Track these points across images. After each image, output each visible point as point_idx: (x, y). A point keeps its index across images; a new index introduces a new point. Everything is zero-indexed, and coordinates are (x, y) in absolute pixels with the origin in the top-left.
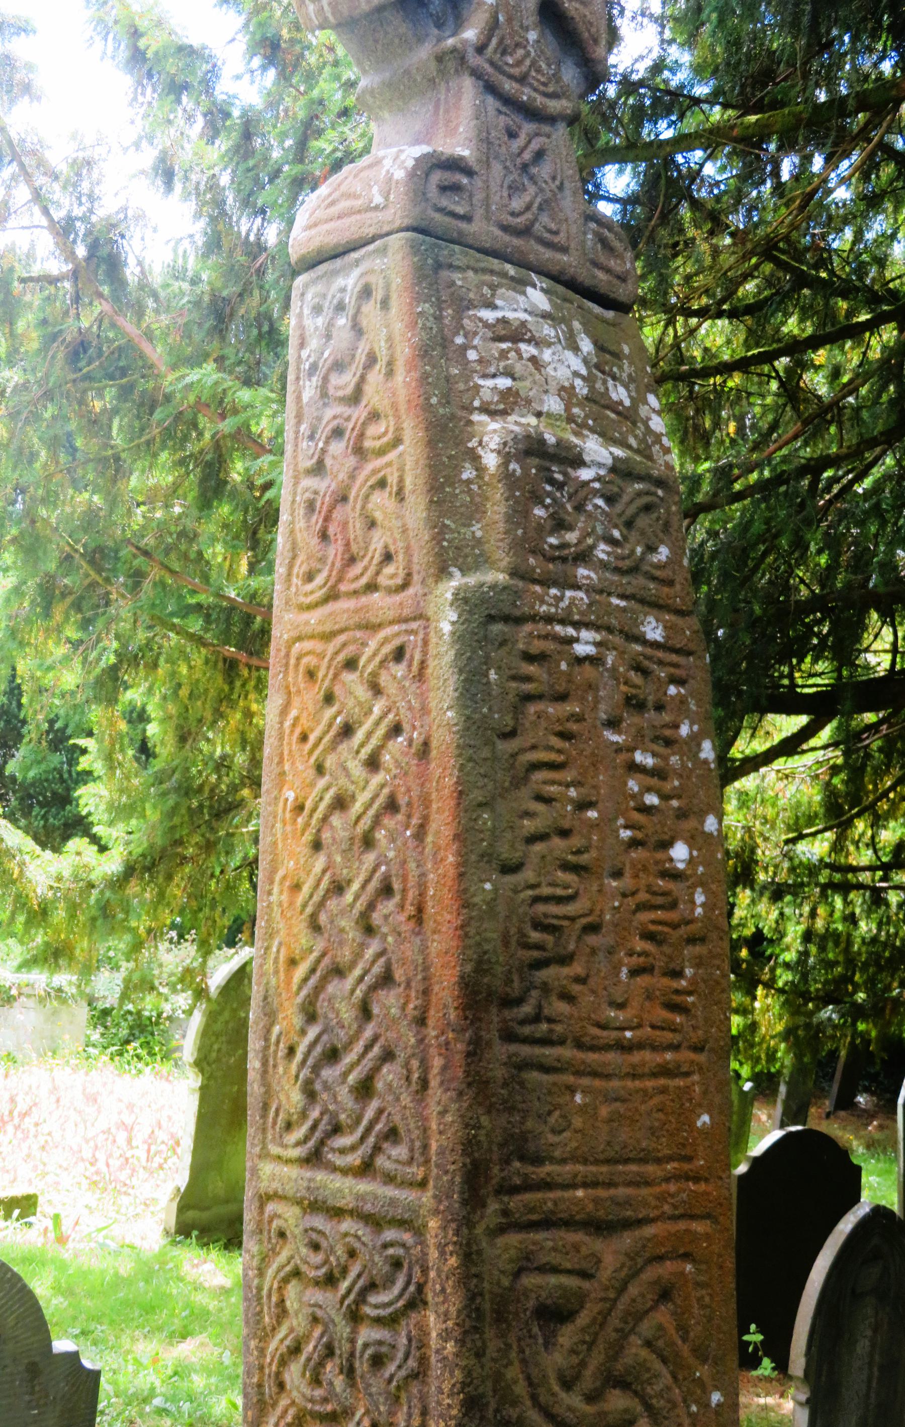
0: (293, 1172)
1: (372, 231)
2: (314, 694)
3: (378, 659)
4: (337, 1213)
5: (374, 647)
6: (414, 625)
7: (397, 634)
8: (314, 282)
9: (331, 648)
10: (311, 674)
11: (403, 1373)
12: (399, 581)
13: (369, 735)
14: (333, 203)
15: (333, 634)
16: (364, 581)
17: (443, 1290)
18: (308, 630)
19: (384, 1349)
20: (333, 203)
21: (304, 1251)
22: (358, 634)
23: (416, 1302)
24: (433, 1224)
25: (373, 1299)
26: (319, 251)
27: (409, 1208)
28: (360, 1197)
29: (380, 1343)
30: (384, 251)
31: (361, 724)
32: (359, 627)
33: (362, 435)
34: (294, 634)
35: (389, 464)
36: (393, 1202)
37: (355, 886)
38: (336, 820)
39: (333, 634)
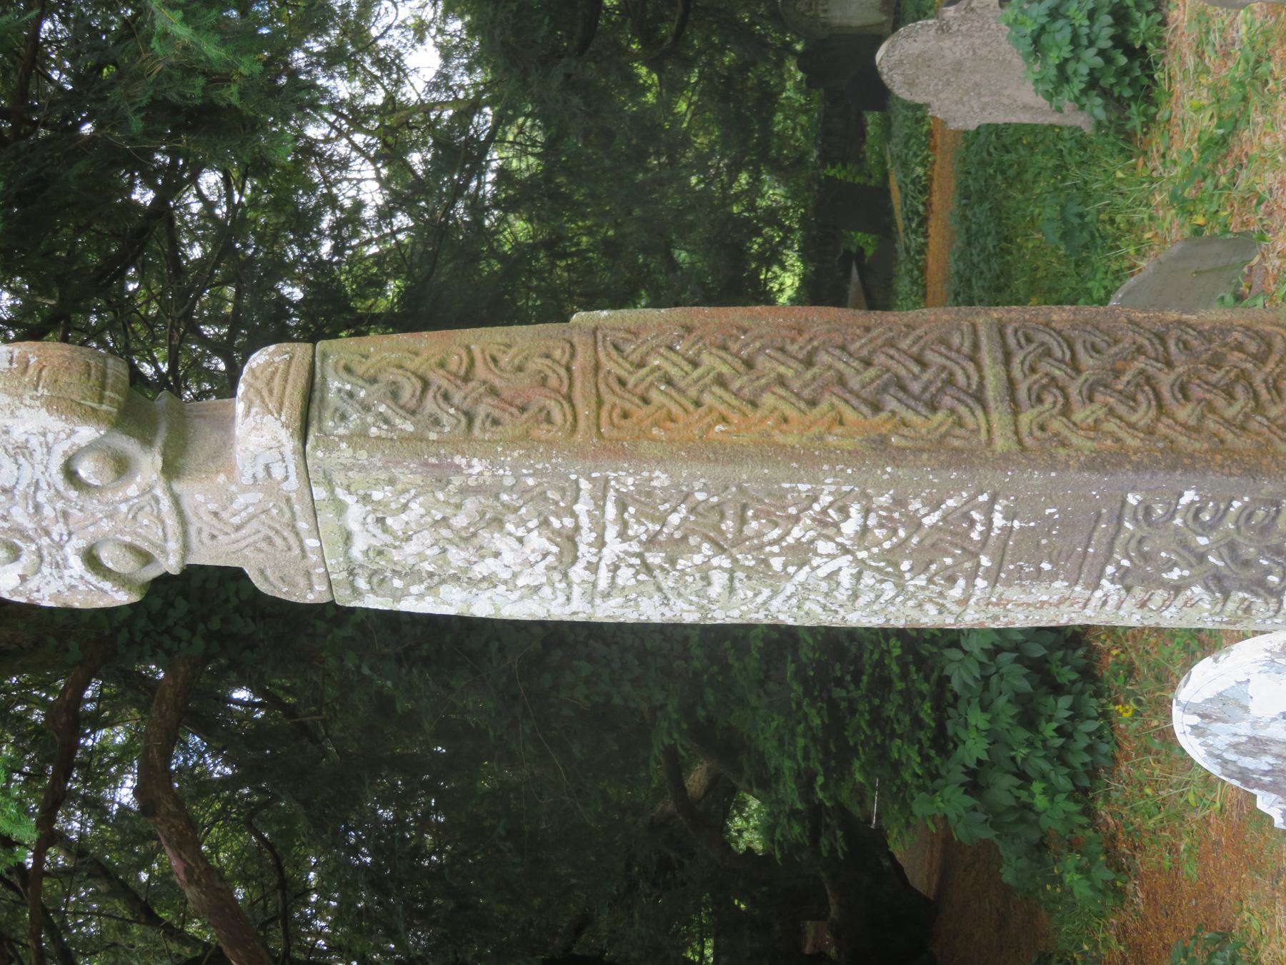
0: (995, 417)
1: (304, 374)
2: (640, 412)
3: (620, 360)
4: (1011, 384)
5: (610, 365)
6: (600, 336)
7: (605, 348)
8: (320, 420)
9: (608, 398)
10: (625, 415)
12: (568, 346)
13: (674, 364)
14: (271, 392)
15: (598, 395)
16: (563, 372)
18: (593, 416)
19: (1088, 346)
20: (271, 392)
21: (1047, 405)
22: (601, 375)
24: (995, 315)
25: (1059, 354)
26: (304, 397)
29: (1085, 348)
30: (325, 356)
31: (666, 373)
32: (596, 375)
33: (456, 375)
34: (594, 430)
35: (483, 351)
36: (989, 338)
37: (782, 369)
38: (736, 385)
39: (598, 395)
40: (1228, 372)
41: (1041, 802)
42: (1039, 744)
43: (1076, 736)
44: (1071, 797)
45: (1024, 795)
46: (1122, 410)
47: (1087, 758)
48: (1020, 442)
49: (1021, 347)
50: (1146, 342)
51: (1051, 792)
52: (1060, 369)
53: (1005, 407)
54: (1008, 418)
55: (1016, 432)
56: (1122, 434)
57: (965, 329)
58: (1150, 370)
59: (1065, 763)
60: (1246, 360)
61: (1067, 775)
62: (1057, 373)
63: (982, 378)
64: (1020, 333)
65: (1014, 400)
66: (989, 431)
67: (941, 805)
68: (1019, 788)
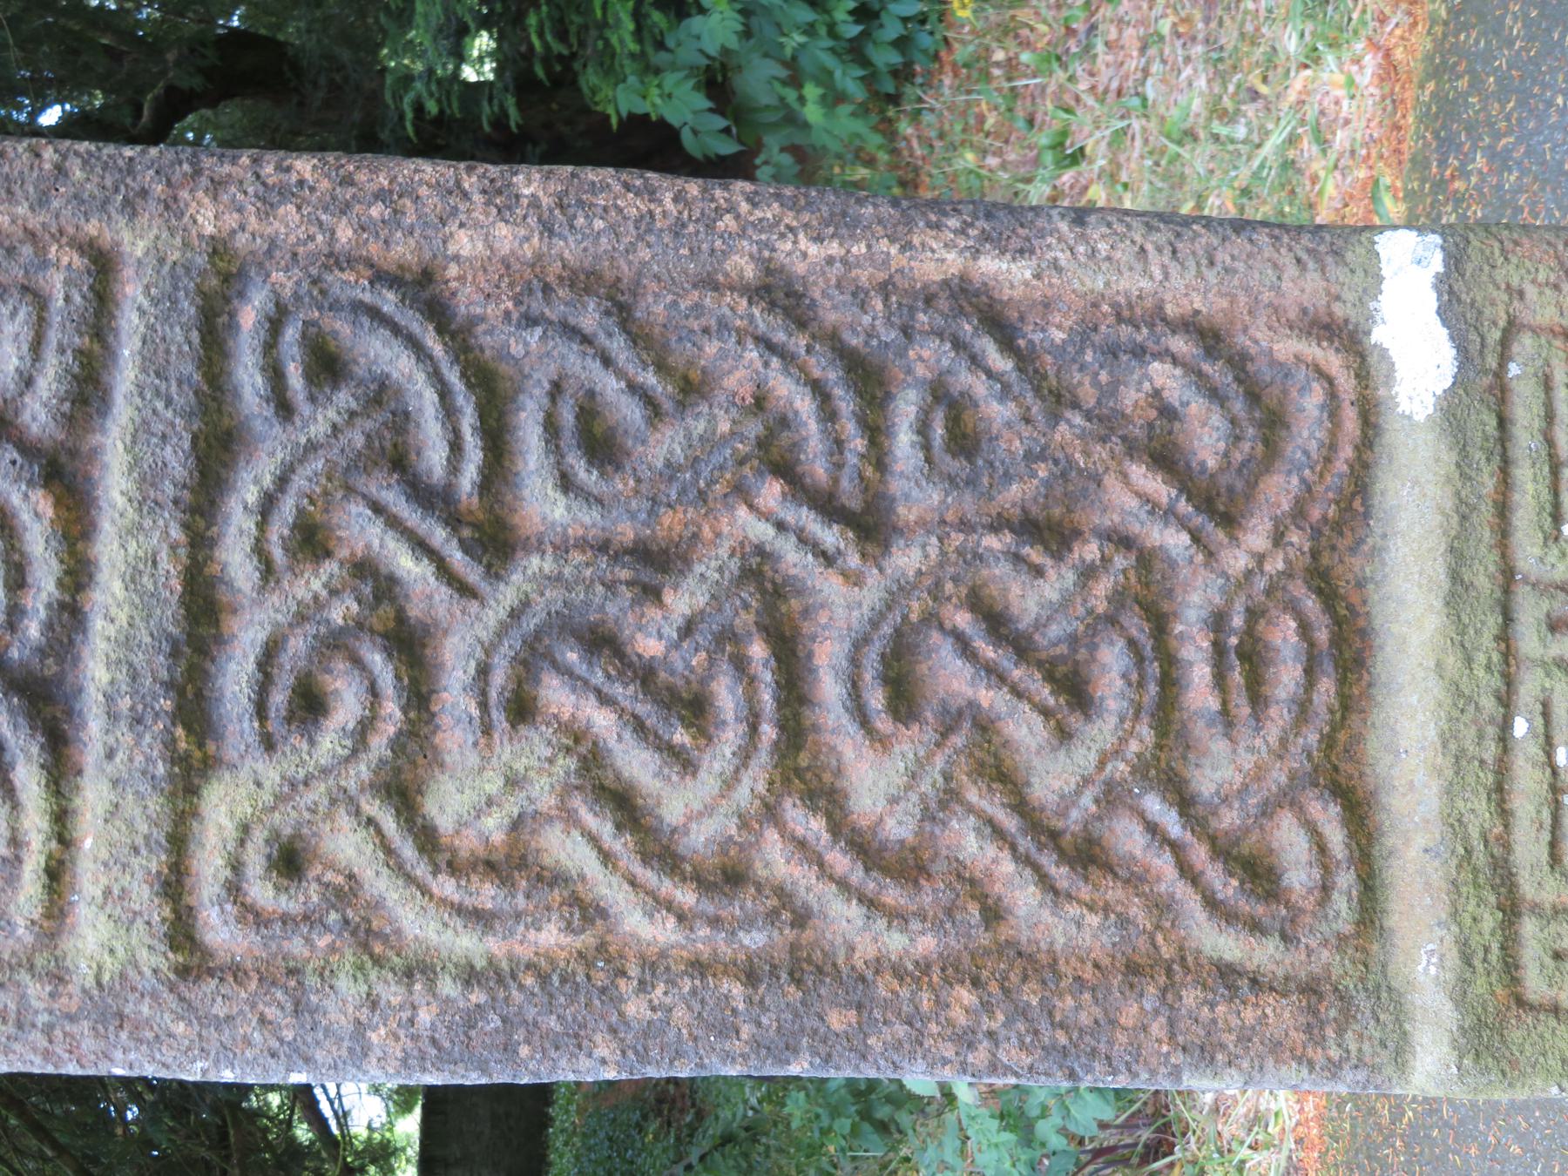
0: (93, 796)
4: (202, 608)
11: (618, 346)
17: (381, 195)
19: (567, 416)
21: (330, 741)
23: (423, 288)
24: (207, 219)
25: (435, 458)
27: (166, 302)
28: (145, 502)
29: (551, 427)
36: (154, 362)
40: (1088, 573)
41: (813, 113)
42: (823, 31)
43: (884, 17)
44: (863, 111)
45: (791, 95)
46: (636, 764)
47: (895, 58)
48: (182, 932)
49: (284, 408)
50: (805, 405)
51: (834, 98)
52: (421, 547)
53: (145, 752)
54: (147, 811)
55: (174, 884)
56: (609, 890)
57: (55, 284)
58: (793, 558)
59: (865, 62)
60: (1168, 515)
61: (862, 79)
62: (407, 565)
63: (78, 576)
64: (291, 333)
65: (193, 708)
66: (56, 874)
67: (658, 101)
68: (784, 83)
